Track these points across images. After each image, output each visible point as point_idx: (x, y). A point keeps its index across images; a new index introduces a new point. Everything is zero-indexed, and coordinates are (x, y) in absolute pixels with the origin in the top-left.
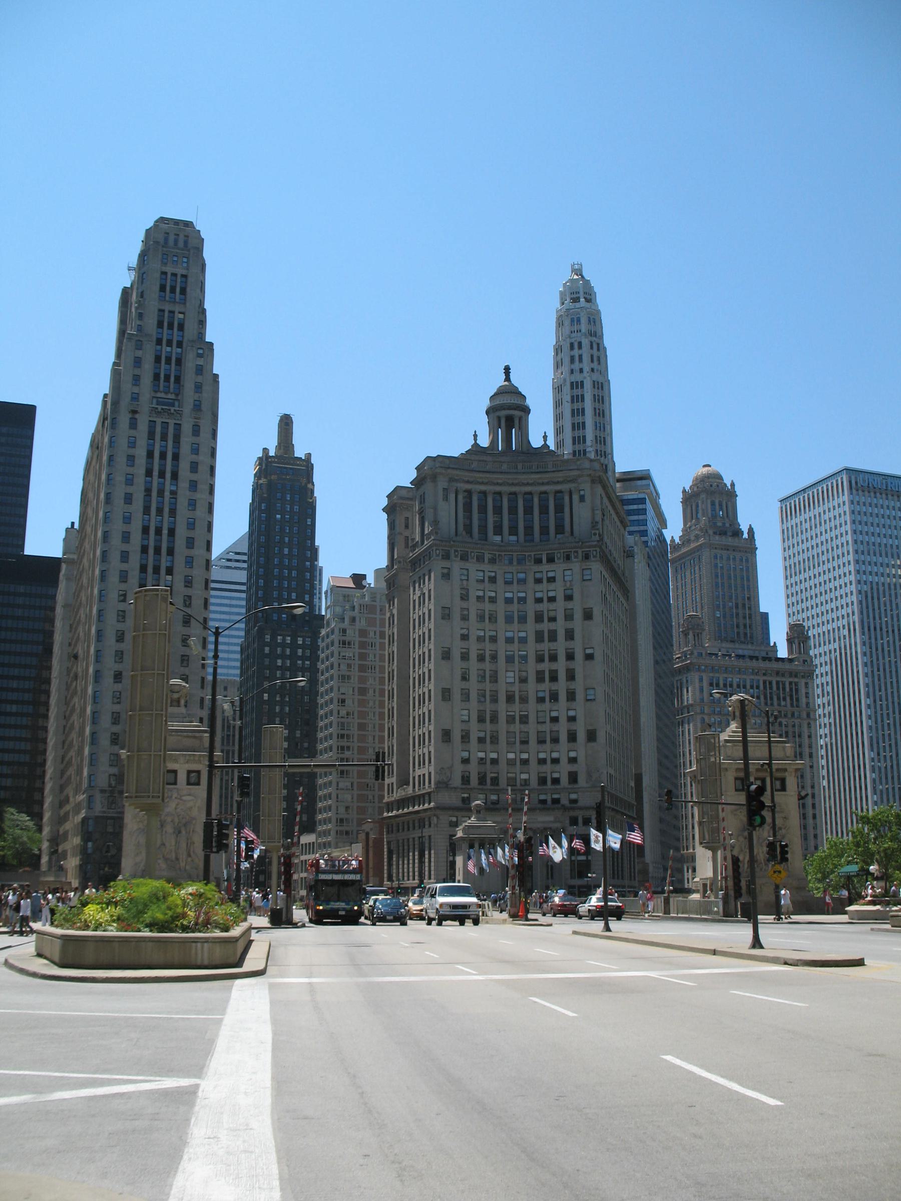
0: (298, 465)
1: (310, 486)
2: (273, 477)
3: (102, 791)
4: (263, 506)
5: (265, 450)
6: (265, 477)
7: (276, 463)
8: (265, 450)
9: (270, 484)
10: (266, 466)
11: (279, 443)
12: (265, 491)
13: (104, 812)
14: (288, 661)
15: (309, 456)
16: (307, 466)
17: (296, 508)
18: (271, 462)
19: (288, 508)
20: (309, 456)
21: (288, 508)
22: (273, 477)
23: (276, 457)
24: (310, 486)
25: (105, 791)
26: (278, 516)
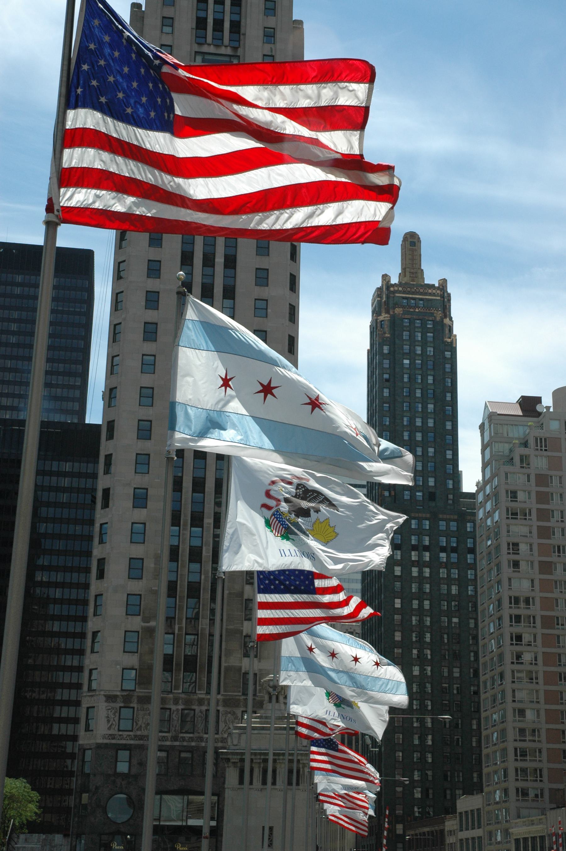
0: (430, 294)
1: (447, 321)
2: (398, 311)
3: (110, 698)
4: (386, 349)
5: (385, 277)
6: (387, 312)
7: (400, 292)
8: (385, 277)
9: (394, 322)
10: (388, 297)
11: (404, 269)
12: (387, 329)
13: (113, 737)
14: (427, 554)
15: (444, 283)
16: (443, 296)
17: (430, 351)
18: (394, 292)
19: (419, 350)
20: (444, 283)
21: (419, 350)
22: (398, 311)
23: (400, 284)
24: (447, 321)
25: (116, 696)
26: (406, 362)
